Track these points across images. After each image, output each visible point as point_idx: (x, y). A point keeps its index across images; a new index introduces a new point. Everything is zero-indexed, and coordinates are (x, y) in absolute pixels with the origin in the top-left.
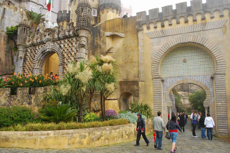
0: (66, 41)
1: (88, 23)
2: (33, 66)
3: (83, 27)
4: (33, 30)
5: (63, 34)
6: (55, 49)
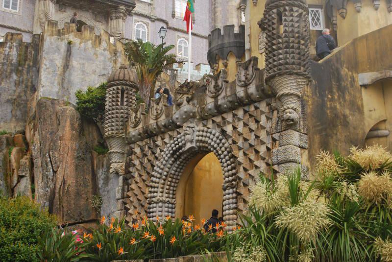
0: (240, 113)
1: (302, 54)
2: (149, 195)
3: (287, 69)
4: (146, 92)
5: (229, 94)
6: (210, 141)
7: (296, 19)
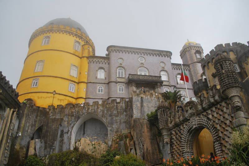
0: (214, 109)
1: (235, 78)
2: (182, 150)
3: (230, 85)
4: (173, 110)
5: (207, 102)
6: (203, 123)
7: (228, 65)
